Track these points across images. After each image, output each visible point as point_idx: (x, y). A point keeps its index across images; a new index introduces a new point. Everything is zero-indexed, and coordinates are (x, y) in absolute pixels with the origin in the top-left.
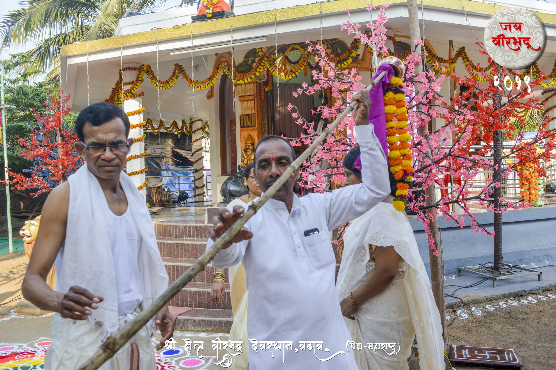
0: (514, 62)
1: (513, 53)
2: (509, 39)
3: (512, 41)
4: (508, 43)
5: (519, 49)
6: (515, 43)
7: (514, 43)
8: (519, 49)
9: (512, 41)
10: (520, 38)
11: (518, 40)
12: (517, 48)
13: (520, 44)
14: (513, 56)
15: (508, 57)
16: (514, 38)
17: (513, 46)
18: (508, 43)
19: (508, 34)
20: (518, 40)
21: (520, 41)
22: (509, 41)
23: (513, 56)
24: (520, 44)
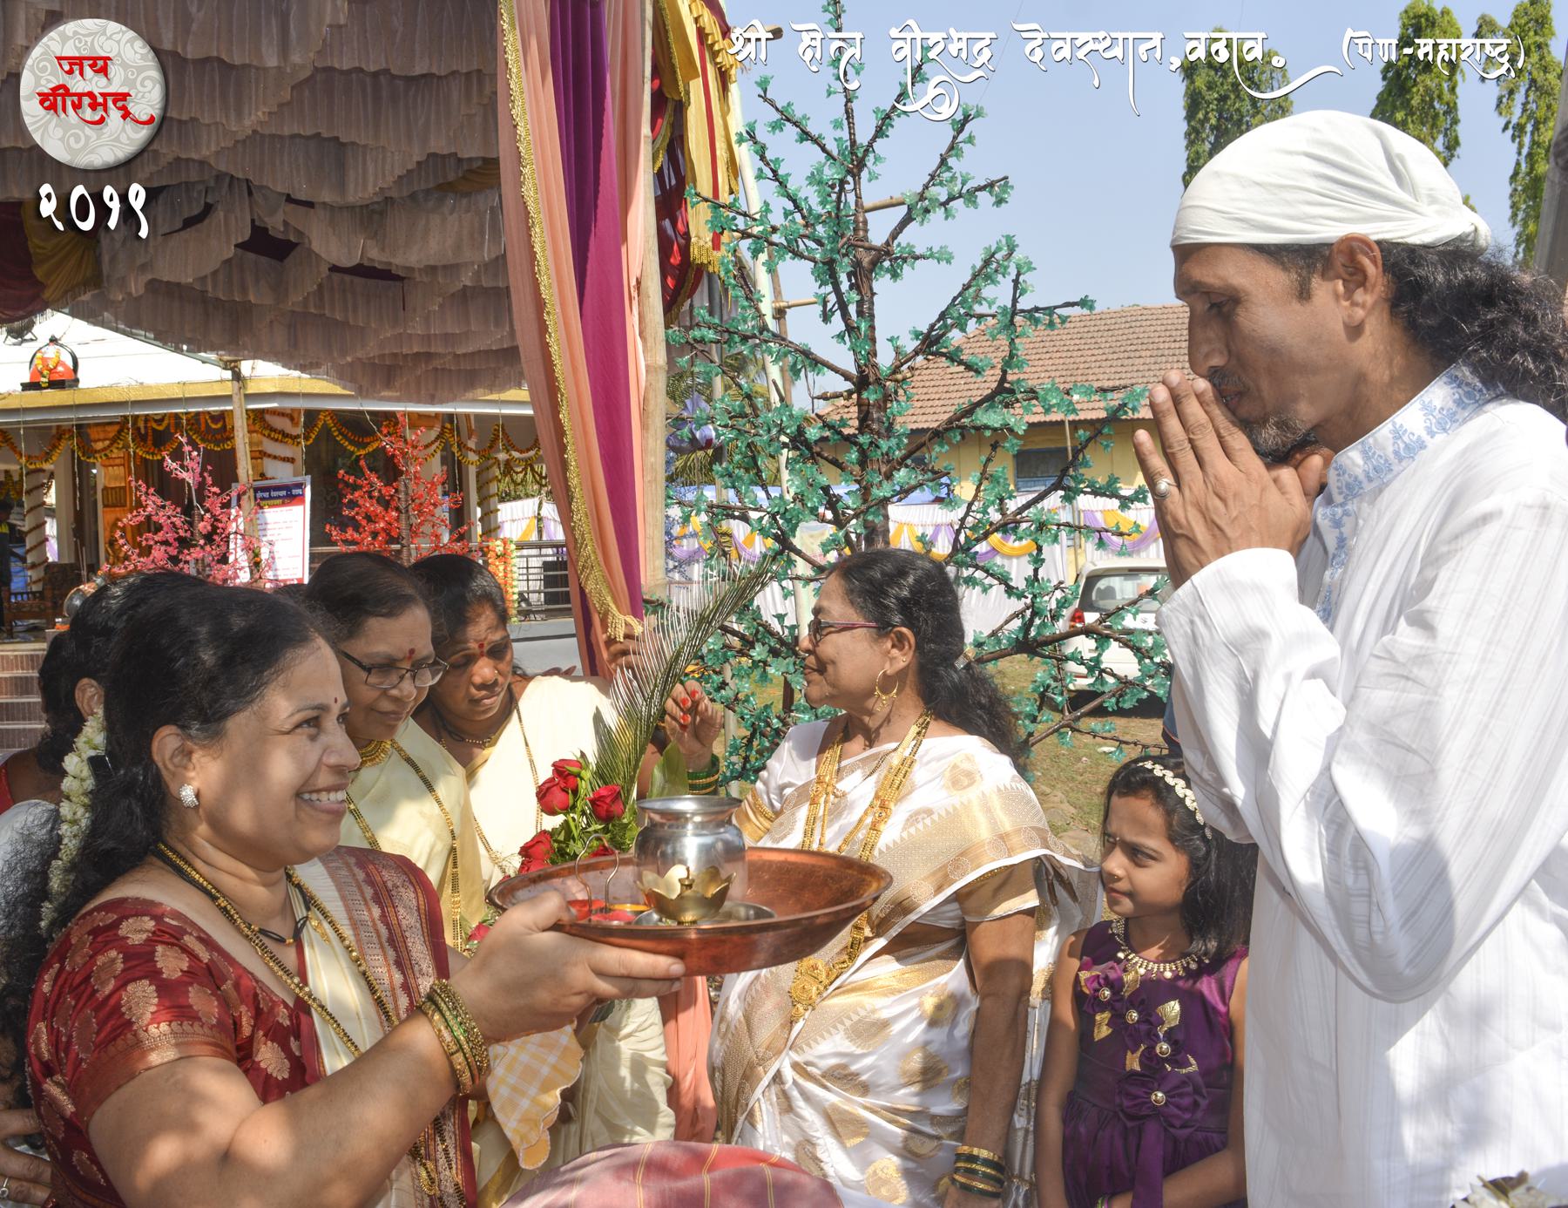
5: (102, 120)
8: (102, 120)
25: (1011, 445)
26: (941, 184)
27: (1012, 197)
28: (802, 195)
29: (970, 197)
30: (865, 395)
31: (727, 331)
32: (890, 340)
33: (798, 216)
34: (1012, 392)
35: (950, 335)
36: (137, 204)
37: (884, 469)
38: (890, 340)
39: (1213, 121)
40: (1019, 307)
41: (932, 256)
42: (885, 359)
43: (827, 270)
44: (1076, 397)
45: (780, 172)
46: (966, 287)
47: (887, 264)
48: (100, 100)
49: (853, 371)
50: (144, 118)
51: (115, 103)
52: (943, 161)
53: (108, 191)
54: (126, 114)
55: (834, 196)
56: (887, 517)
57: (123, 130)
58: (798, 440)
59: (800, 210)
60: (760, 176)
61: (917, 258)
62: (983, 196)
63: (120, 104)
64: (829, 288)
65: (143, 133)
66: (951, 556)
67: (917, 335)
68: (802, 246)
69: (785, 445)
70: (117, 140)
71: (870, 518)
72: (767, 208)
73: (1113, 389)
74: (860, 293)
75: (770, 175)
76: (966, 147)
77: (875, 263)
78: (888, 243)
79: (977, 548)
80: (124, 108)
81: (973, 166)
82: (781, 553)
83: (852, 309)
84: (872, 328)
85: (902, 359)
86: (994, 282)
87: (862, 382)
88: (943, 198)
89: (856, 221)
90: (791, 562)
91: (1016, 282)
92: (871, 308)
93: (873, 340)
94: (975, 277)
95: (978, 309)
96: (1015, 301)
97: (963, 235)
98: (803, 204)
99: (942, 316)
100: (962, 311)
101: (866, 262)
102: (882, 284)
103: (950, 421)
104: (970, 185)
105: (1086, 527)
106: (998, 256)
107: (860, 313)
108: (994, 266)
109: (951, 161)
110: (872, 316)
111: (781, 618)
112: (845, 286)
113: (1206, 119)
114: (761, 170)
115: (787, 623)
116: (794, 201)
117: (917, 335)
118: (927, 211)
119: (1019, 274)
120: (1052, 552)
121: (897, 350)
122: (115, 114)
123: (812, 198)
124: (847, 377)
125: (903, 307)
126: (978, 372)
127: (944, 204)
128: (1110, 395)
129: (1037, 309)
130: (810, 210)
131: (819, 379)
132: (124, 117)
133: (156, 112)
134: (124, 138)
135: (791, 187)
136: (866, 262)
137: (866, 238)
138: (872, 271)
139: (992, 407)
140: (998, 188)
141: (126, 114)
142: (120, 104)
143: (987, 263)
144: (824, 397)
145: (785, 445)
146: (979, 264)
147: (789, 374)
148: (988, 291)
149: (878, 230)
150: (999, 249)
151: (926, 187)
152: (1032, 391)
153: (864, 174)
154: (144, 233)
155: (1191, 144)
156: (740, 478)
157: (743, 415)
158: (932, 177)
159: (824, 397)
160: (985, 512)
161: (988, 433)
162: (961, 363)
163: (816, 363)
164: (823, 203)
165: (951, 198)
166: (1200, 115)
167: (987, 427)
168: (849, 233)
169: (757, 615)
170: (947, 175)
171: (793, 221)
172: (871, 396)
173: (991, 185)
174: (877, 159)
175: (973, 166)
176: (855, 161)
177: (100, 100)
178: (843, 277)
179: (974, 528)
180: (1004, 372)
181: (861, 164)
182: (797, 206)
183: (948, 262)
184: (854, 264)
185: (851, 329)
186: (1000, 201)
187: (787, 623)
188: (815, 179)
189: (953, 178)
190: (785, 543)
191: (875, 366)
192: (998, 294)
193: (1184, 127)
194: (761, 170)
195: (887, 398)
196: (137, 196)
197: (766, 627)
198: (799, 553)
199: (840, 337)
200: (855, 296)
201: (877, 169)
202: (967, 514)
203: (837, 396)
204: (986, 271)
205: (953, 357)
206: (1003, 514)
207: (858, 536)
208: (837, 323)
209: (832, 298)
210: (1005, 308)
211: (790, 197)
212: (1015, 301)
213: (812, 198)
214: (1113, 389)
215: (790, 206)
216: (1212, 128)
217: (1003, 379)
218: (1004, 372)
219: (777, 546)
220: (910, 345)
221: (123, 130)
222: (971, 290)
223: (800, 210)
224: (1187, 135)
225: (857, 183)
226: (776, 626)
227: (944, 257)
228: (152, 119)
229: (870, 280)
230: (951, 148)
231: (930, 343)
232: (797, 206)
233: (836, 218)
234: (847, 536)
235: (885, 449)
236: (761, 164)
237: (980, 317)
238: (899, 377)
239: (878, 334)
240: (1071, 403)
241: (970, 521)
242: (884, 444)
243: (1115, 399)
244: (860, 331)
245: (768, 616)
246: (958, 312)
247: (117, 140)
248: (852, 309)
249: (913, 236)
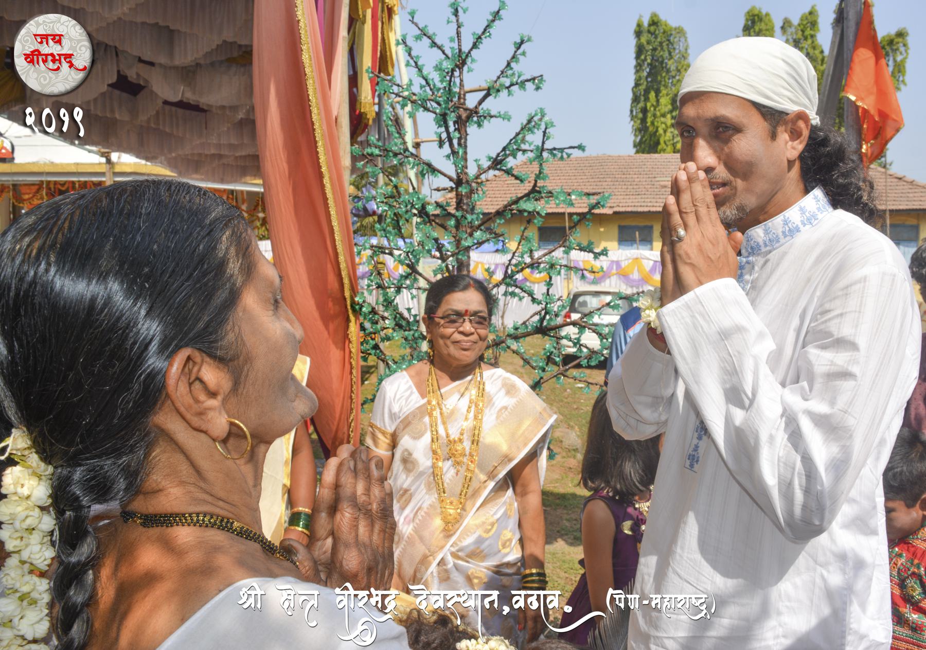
25: (538, 222)
26: (507, 76)
27: (544, 86)
28: (430, 77)
29: (522, 84)
30: (460, 189)
31: (386, 150)
32: (476, 161)
33: (428, 89)
34: (539, 192)
35: (507, 160)
36: (78, 119)
37: (469, 231)
38: (476, 161)
39: (649, 61)
40: (546, 146)
41: (500, 116)
42: (472, 170)
43: (443, 119)
44: (573, 197)
45: (419, 63)
46: (518, 134)
47: (475, 119)
48: (57, 57)
49: (454, 176)
52: (508, 64)
53: (63, 111)
54: (71, 65)
55: (448, 78)
56: (469, 257)
57: (70, 74)
58: (423, 212)
59: (429, 85)
60: (408, 65)
61: (492, 117)
62: (529, 85)
64: (443, 129)
66: (503, 280)
67: (490, 158)
68: (429, 105)
69: (415, 215)
70: (66, 79)
71: (460, 257)
72: (410, 83)
73: (594, 194)
74: (460, 133)
75: (414, 64)
76: (521, 58)
77: (469, 118)
78: (476, 107)
79: (517, 276)
80: (70, 62)
81: (525, 68)
82: (410, 274)
83: (455, 142)
84: (465, 153)
85: (481, 171)
86: (533, 132)
87: (459, 182)
88: (507, 84)
89: (459, 94)
90: (416, 280)
91: (545, 132)
92: (465, 142)
93: (466, 160)
94: (522, 129)
95: (523, 147)
96: (543, 143)
97: (516, 106)
98: (431, 82)
99: (504, 149)
100: (515, 147)
101: (464, 116)
102: (472, 129)
103: (506, 206)
104: (523, 78)
105: (575, 267)
106: (536, 119)
107: (459, 144)
108: (533, 123)
109: (513, 65)
110: (466, 147)
111: (409, 310)
112: (452, 129)
113: (645, 59)
114: (408, 61)
115: (413, 312)
116: (426, 80)
117: (490, 158)
118: (498, 91)
119: (546, 128)
120: (558, 280)
121: (479, 166)
122: (65, 65)
123: (435, 77)
124: (451, 179)
125: (483, 142)
126: (522, 181)
127: (508, 88)
128: (591, 197)
129: (555, 149)
130: (434, 85)
131: (435, 180)
132: (70, 67)
134: (70, 78)
135: (425, 73)
136: (464, 116)
137: (464, 104)
138: (467, 121)
139: (529, 200)
140: (537, 81)
141: (71, 65)
143: (529, 122)
144: (438, 190)
145: (415, 215)
146: (525, 122)
147: (420, 178)
148: (529, 137)
149: (471, 101)
150: (536, 115)
151: (499, 78)
152: (550, 192)
153: (465, 68)
154: (82, 134)
155: (637, 72)
156: (390, 232)
157: (392, 197)
158: (502, 72)
159: (438, 190)
160: (522, 257)
161: (526, 214)
162: (513, 175)
163: (433, 170)
164: (442, 81)
165: (512, 85)
166: (643, 57)
167: (525, 211)
168: (455, 99)
169: (396, 308)
170: (510, 72)
171: (425, 91)
172: (463, 190)
173: (534, 79)
174: (473, 60)
175: (525, 68)
176: (461, 61)
177: (57, 57)
178: (451, 124)
179: (516, 265)
180: (536, 181)
181: (464, 63)
182: (427, 83)
183: (509, 120)
184: (458, 117)
185: (454, 153)
186: (538, 88)
187: (413, 312)
188: (438, 68)
189: (513, 74)
190: (413, 268)
191: (466, 174)
192: (535, 139)
193: (634, 62)
194: (408, 61)
195: (472, 191)
196: (78, 114)
197: (401, 315)
198: (420, 275)
199: (448, 157)
200: (457, 135)
201: (473, 66)
202: (512, 258)
203: (444, 189)
204: (529, 126)
205: (509, 172)
206: (532, 259)
207: (453, 267)
208: (447, 149)
209: (444, 136)
210: (538, 147)
211: (424, 78)
212: (543, 143)
213: (435, 77)
214: (594, 194)
215: (424, 83)
216: (648, 64)
217: (535, 185)
218: (536, 181)
219: (409, 270)
220: (486, 164)
221: (70, 74)
222: (520, 136)
223: (429, 85)
224: (636, 67)
225: (461, 73)
226: (406, 314)
227: (506, 117)
229: (466, 127)
230: (513, 57)
231: (497, 163)
232: (427, 83)
233: (449, 91)
234: (447, 267)
235: (469, 220)
236: (409, 58)
237: (524, 151)
238: (479, 181)
239: (469, 157)
240: (571, 200)
241: (514, 262)
242: (469, 217)
243: (593, 200)
244: (458, 154)
245: (402, 309)
246: (512, 148)
247: (66, 79)
248: (455, 142)
249: (491, 105)
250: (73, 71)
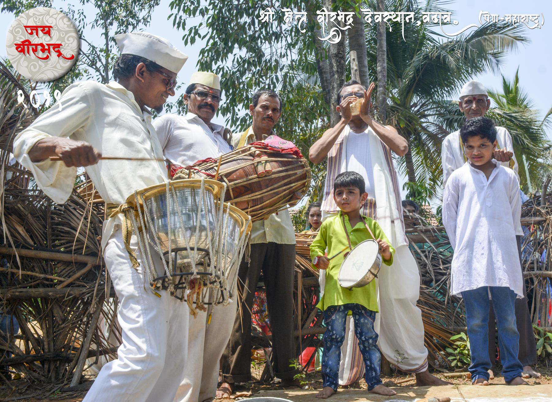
0: (42, 73)
1: (41, 62)
2: (36, 45)
3: (39, 48)
4: (35, 51)
5: (47, 57)
6: (43, 50)
7: (41, 50)
8: (47, 57)
9: (39, 48)
10: (48, 45)
11: (47, 47)
12: (45, 56)
13: (49, 52)
14: (40, 66)
15: (35, 68)
16: (42, 45)
17: (41, 54)
18: (35, 51)
19: (35, 40)
20: (47, 47)
21: (49, 48)
22: (36, 48)
23: (40, 66)
24: (49, 52)
50: (69, 56)
51: (54, 49)
54: (60, 54)
57: (58, 62)
63: (56, 49)
65: (68, 64)
70: (55, 67)
122: (54, 54)
132: (59, 56)
133: (74, 54)
134: (58, 66)
141: (60, 54)
142: (56, 49)
221: (58, 62)
228: (72, 57)
247: (55, 67)
250: (61, 60)
